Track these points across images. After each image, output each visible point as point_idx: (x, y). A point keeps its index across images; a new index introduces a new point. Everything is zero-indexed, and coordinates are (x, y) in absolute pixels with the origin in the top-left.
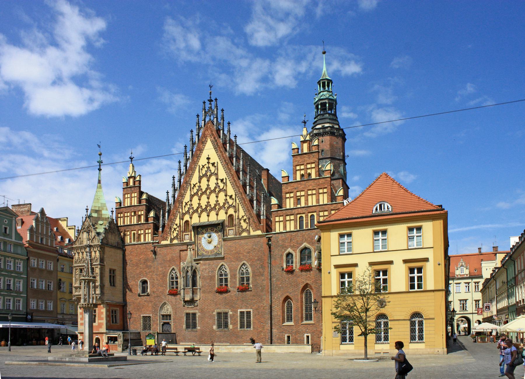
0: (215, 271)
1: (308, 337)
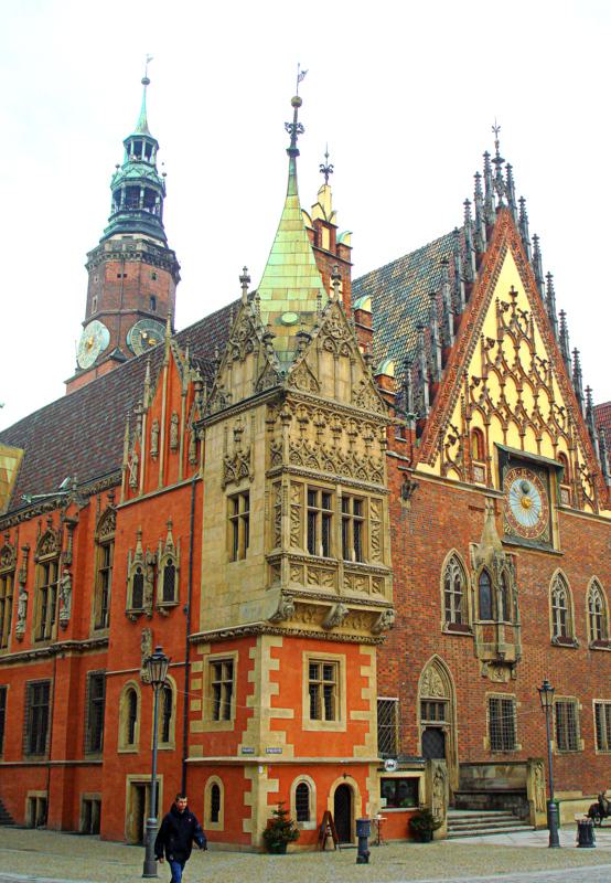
0: (547, 586)
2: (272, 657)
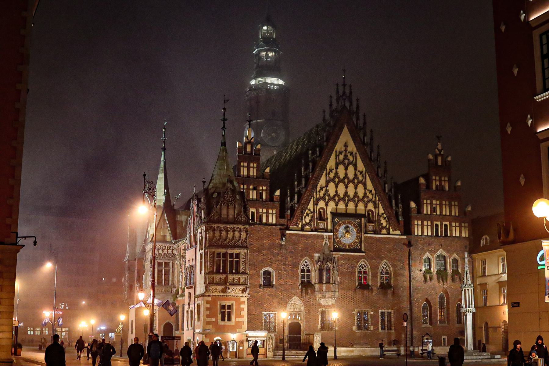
0: (356, 267)
1: (444, 339)
2: (207, 303)
